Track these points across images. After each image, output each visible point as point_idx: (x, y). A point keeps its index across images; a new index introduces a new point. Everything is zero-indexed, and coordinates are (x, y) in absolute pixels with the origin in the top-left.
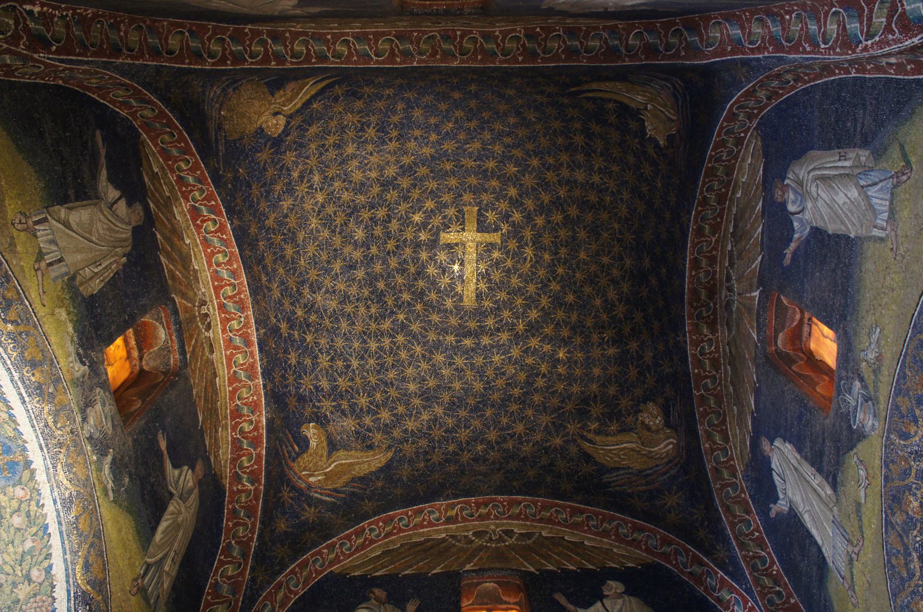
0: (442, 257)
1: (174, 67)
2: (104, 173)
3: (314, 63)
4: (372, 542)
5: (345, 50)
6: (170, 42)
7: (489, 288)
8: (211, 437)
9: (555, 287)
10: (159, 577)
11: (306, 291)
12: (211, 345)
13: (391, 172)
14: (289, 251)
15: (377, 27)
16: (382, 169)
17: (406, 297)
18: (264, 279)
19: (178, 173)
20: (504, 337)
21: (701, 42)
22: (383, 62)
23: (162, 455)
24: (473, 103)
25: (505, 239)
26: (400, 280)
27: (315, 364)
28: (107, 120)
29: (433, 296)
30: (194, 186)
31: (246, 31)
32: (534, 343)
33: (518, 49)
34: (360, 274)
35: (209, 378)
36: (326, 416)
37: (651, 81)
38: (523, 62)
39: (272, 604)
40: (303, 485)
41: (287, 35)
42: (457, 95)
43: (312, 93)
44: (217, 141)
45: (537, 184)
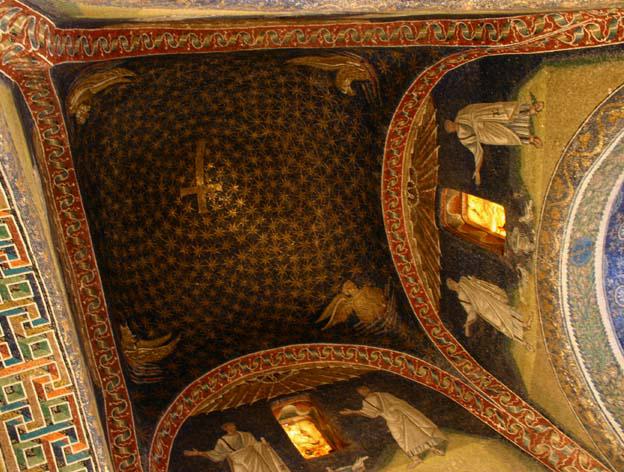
0: (220, 173)
4: (331, 29)
5: (324, 352)
7: (186, 154)
8: (431, 132)
9: (143, 170)
10: (515, 121)
11: (329, 170)
12: (411, 174)
13: (263, 237)
14: (339, 200)
16: (270, 242)
17: (249, 148)
18: (363, 195)
20: (179, 126)
23: (481, 172)
24: (225, 301)
25: (178, 193)
26: (254, 160)
27: (331, 125)
28: (458, 331)
29: (228, 146)
32: (157, 127)
34: (285, 170)
35: (418, 161)
36: (331, 92)
39: (432, 33)
40: (367, 65)
42: (236, 307)
43: (328, 308)
44: (391, 293)
45: (165, 243)
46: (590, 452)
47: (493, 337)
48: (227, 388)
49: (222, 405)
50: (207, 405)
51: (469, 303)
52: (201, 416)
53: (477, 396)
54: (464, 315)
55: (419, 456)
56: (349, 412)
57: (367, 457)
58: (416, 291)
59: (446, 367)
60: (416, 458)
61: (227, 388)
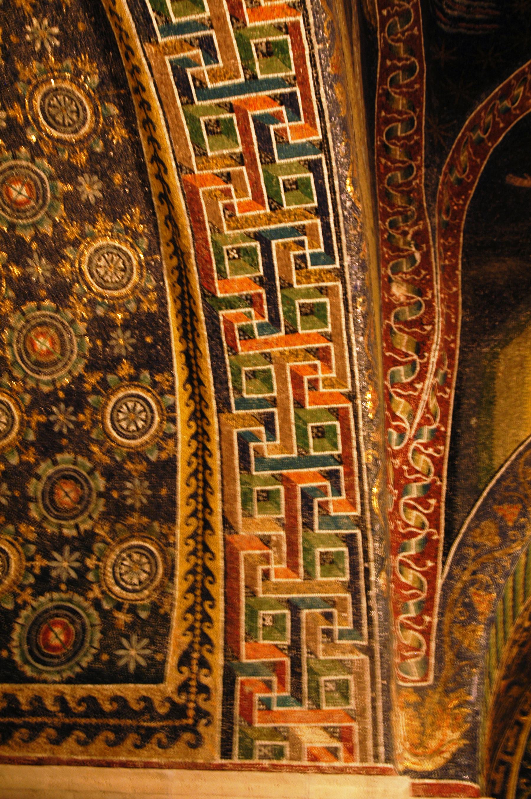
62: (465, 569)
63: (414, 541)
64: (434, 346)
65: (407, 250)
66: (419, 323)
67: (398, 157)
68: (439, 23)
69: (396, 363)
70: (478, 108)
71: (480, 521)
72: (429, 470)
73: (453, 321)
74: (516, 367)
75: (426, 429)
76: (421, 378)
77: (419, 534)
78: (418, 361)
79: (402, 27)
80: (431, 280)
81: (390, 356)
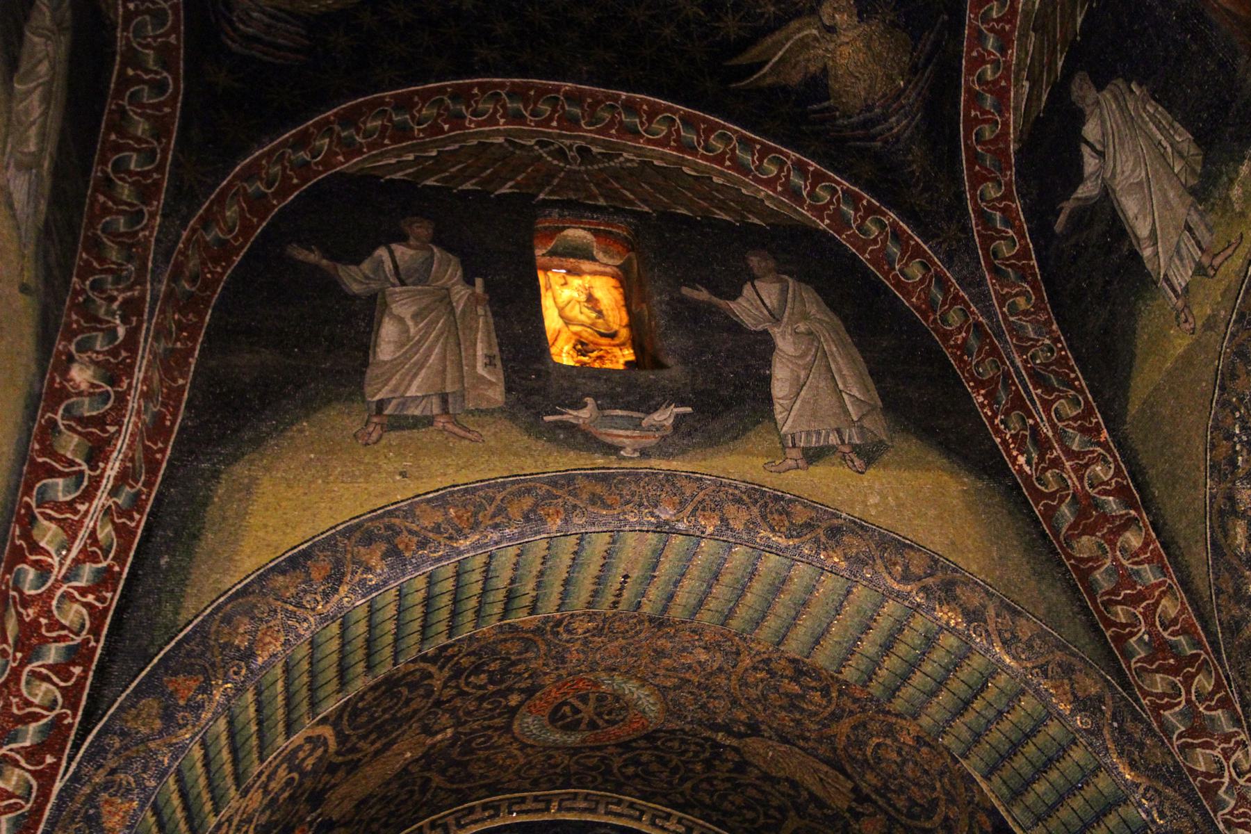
1: (930, 248)
2: (1081, 192)
3: (759, 142)
6: (920, 276)
15: (662, 157)
19: (1002, 60)
21: (245, 189)
22: (669, 109)
28: (1041, 215)
30: (992, 30)
31: (827, 221)
33: (476, 102)
37: (269, 26)
38: (472, 86)
41: (779, 189)
43: (769, 41)
44: (928, 61)
46: (1192, 602)
47: (1115, 257)
48: (453, 140)
49: (427, 173)
50: (394, 162)
51: (1101, 155)
52: (366, 182)
53: (1007, 375)
54: (1075, 175)
55: (805, 451)
56: (703, 295)
57: (689, 409)
58: (989, 76)
59: (973, 282)
60: (794, 453)
61: (453, 140)
62: (101, 766)
63: (33, 727)
64: (115, 454)
65: (109, 322)
66: (100, 421)
67: (124, 197)
68: (223, 37)
69: (52, 473)
70: (257, 154)
71: (139, 699)
72: (83, 626)
73: (168, 423)
74: (240, 491)
75: (88, 569)
76: (88, 496)
77: (43, 716)
78: (87, 472)
79: (153, 30)
80: (132, 366)
81: (45, 463)
